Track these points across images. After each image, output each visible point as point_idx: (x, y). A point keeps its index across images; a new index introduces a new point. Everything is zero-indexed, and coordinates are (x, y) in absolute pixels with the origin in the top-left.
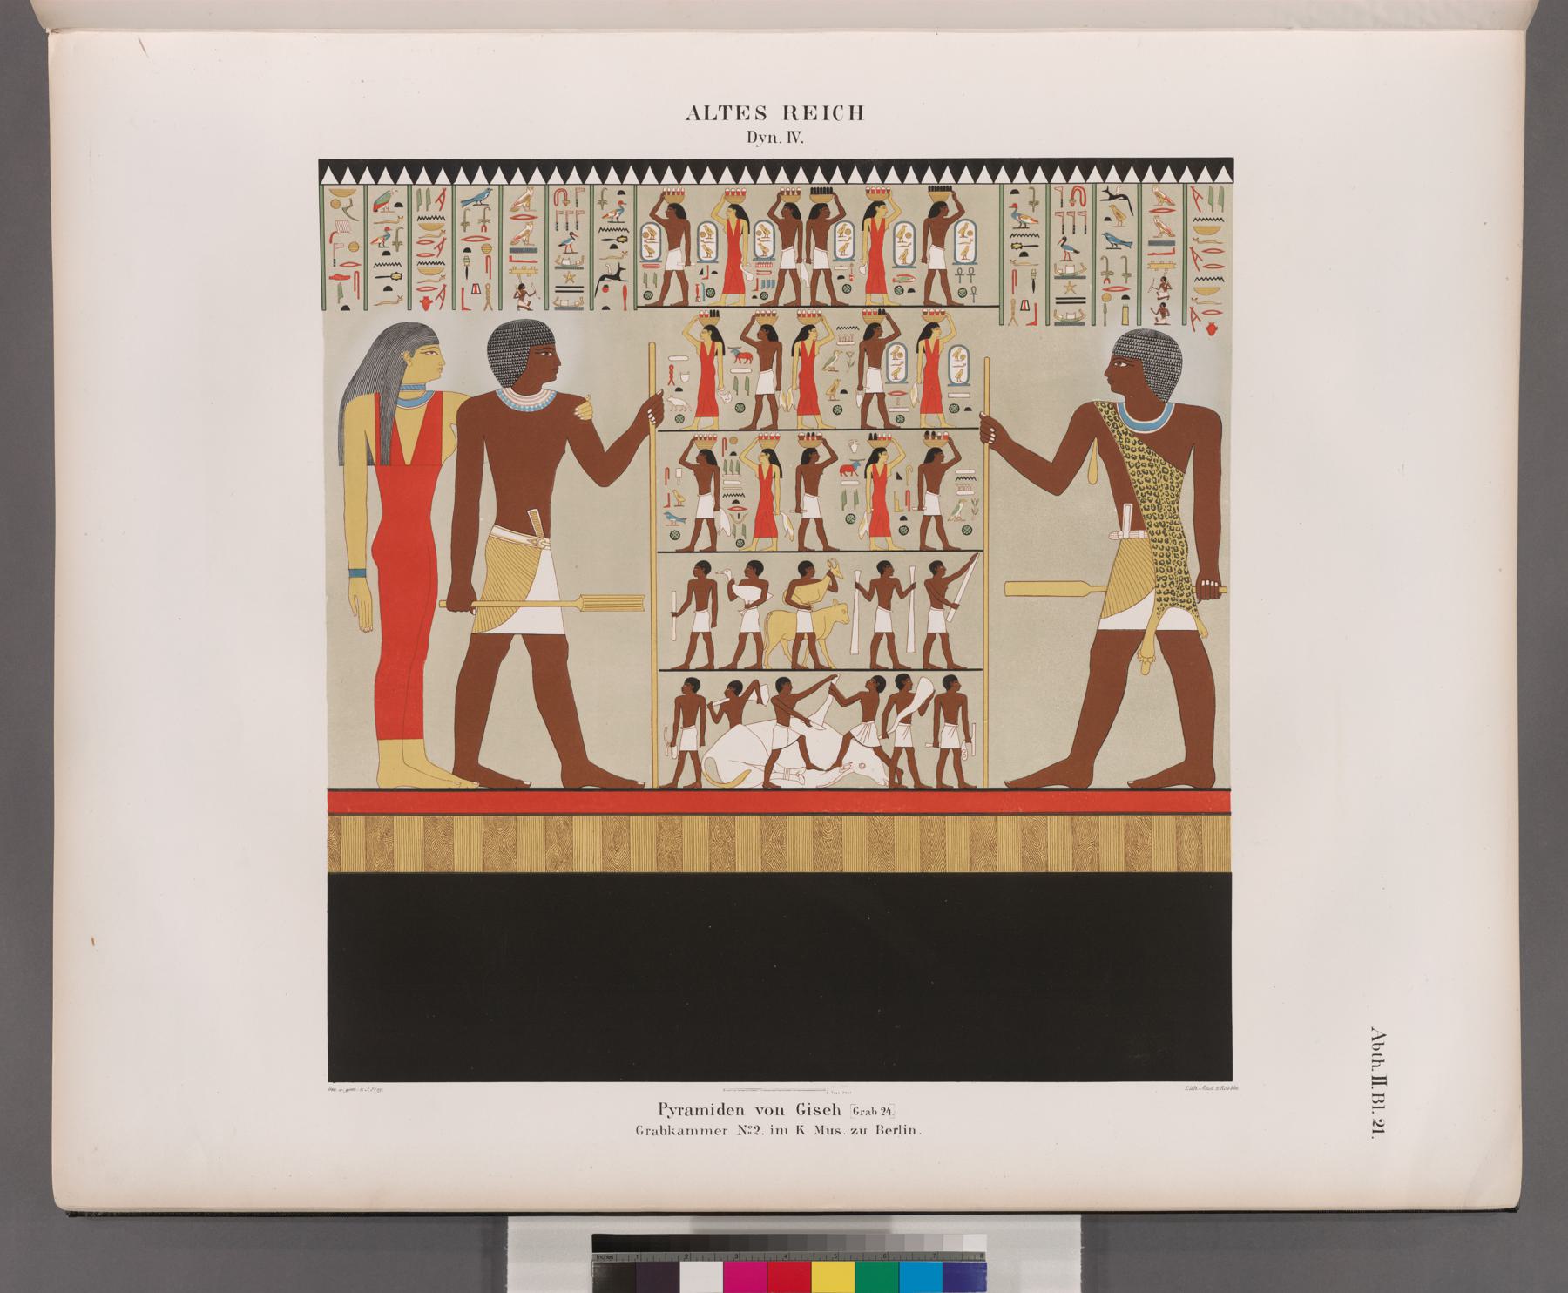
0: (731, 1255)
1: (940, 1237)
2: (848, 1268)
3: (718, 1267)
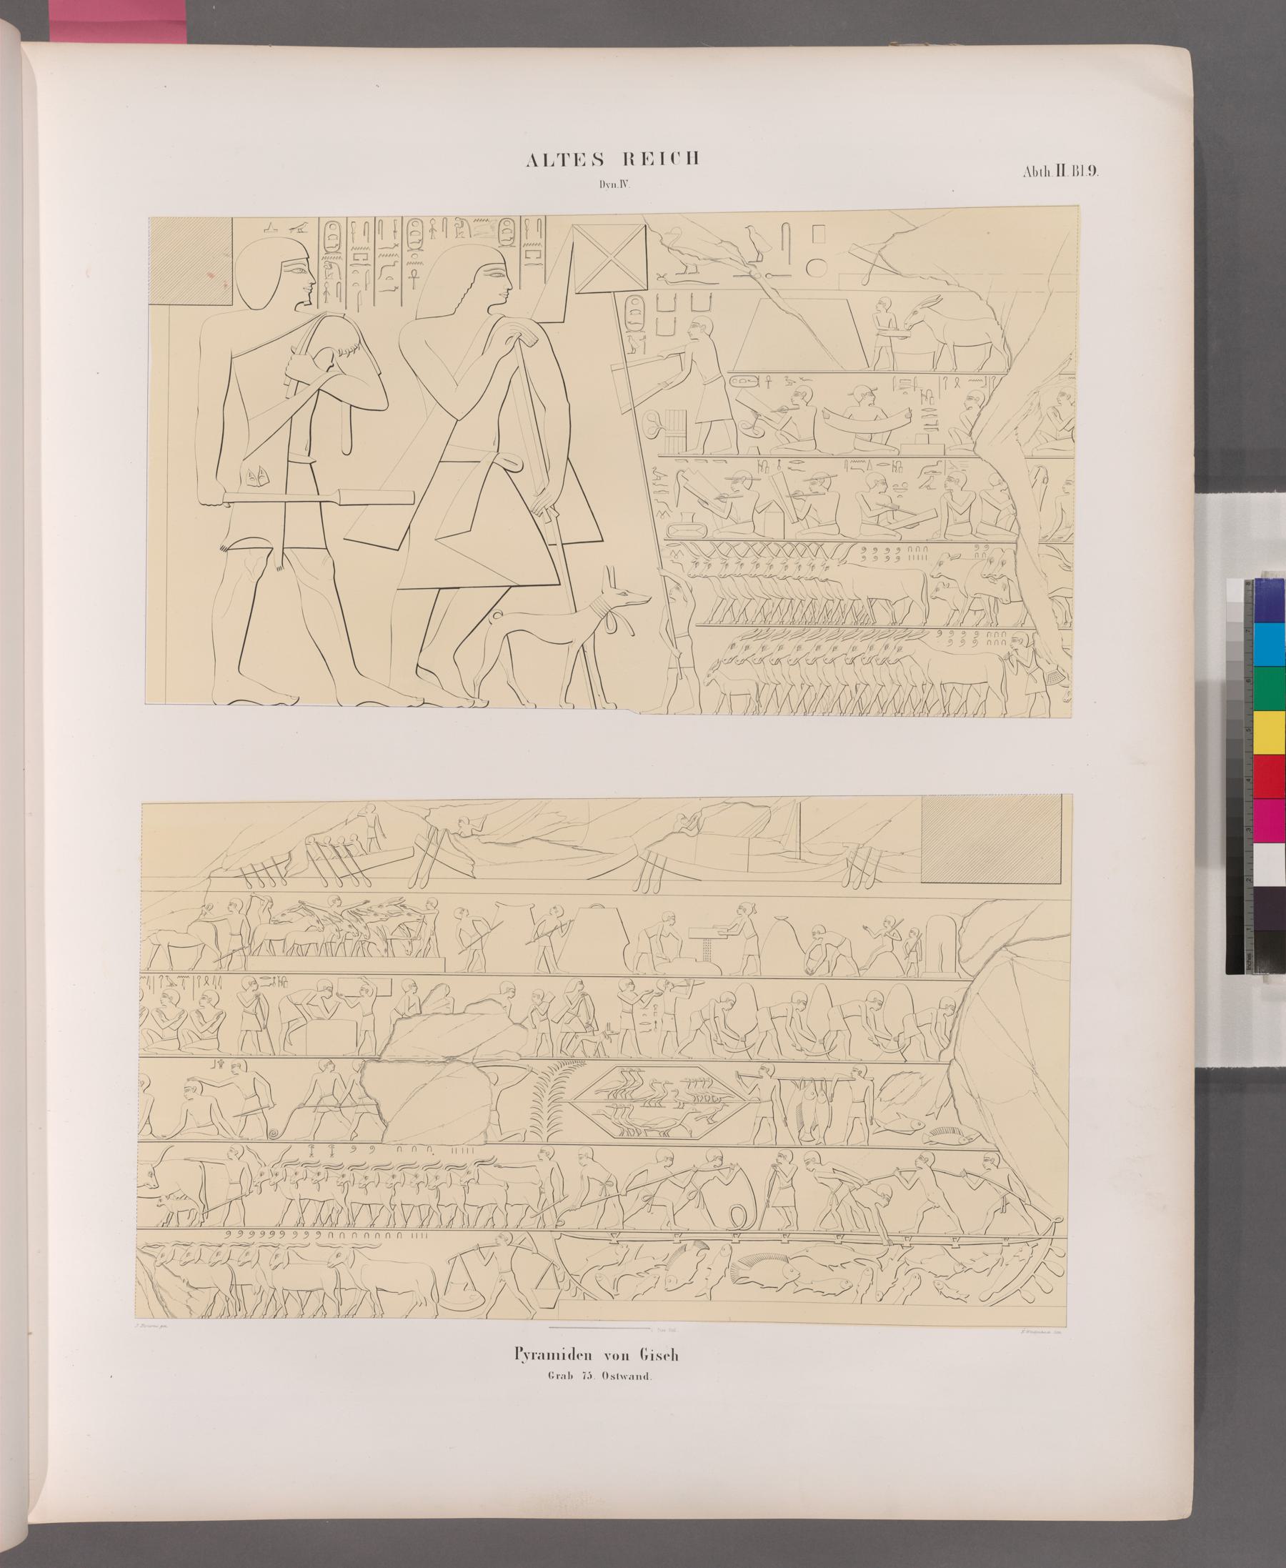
0: (1247, 835)
1: (1229, 625)
2: (1258, 716)
3: (1256, 845)
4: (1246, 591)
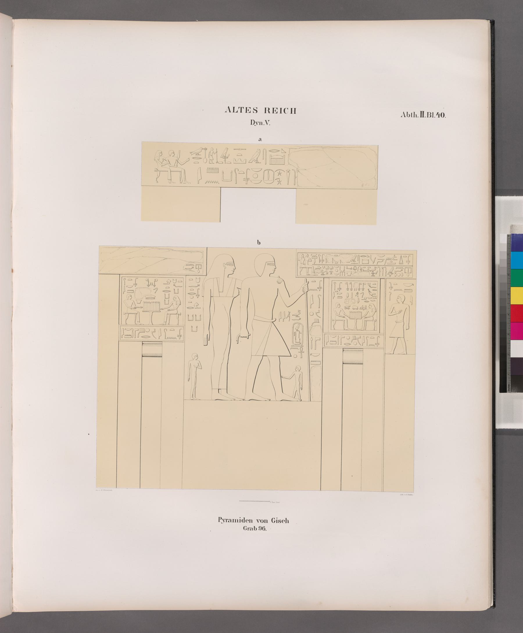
0: (508, 337)
3: (511, 341)
4: (508, 239)
